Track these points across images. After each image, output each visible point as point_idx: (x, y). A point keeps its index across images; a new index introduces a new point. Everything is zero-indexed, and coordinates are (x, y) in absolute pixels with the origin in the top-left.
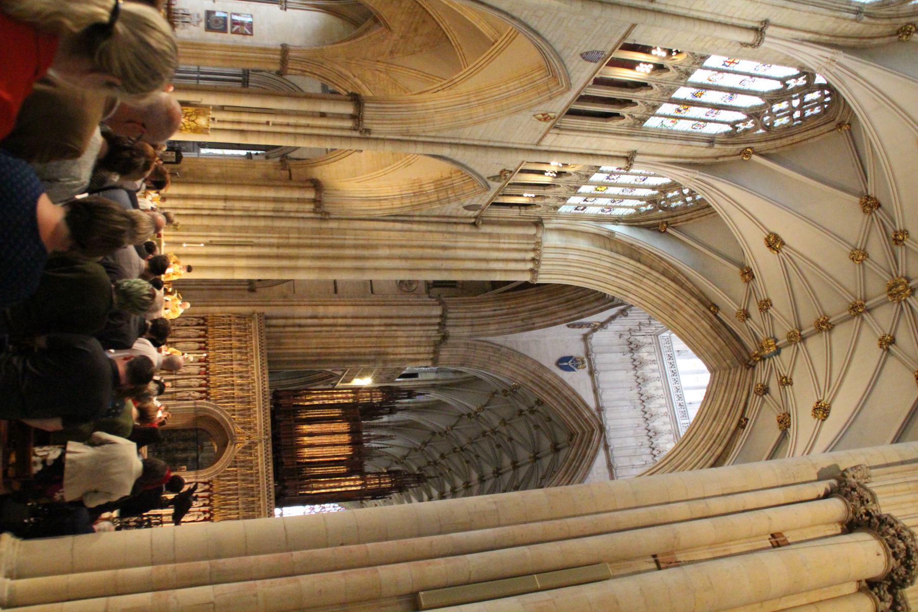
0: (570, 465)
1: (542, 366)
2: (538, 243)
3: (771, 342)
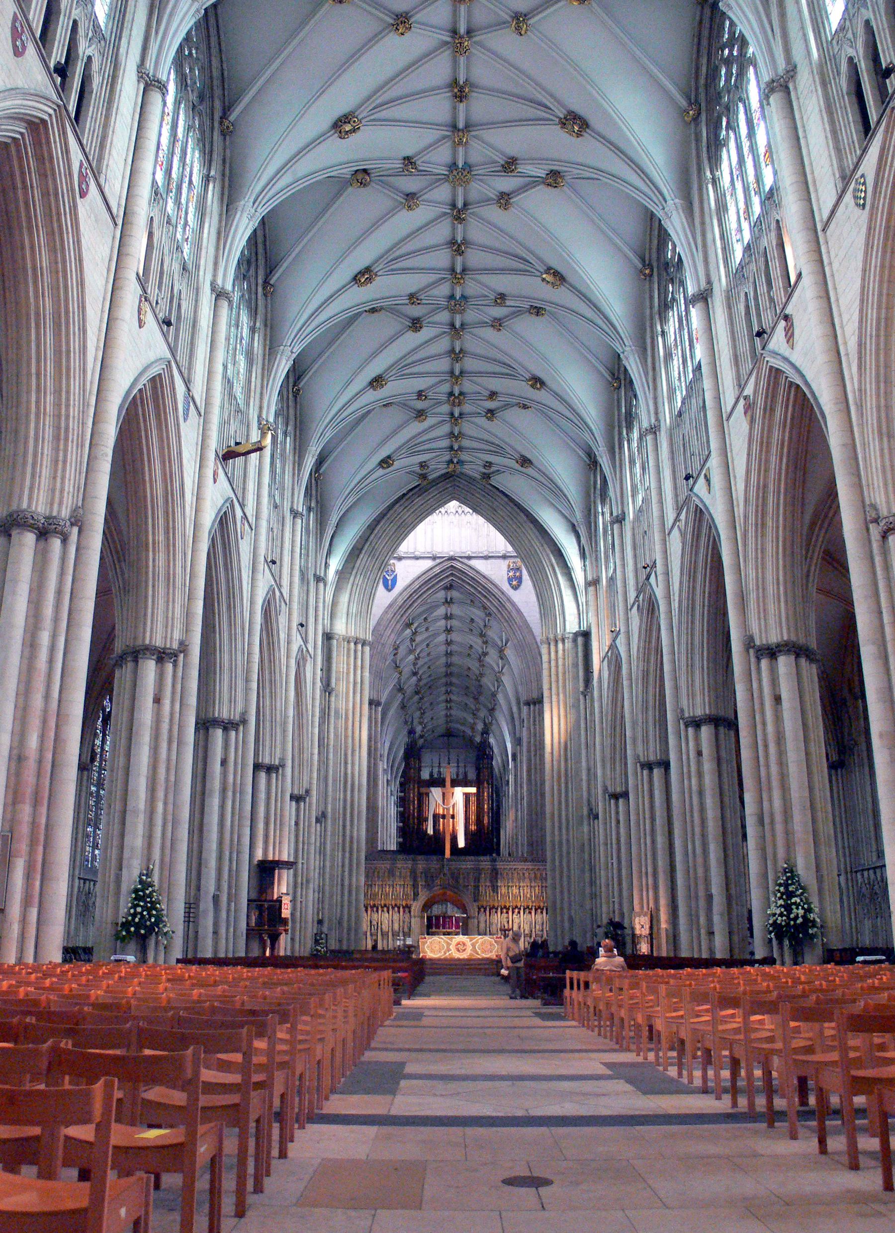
0: (480, 592)
1: (390, 606)
2: (344, 640)
3: (452, 466)
